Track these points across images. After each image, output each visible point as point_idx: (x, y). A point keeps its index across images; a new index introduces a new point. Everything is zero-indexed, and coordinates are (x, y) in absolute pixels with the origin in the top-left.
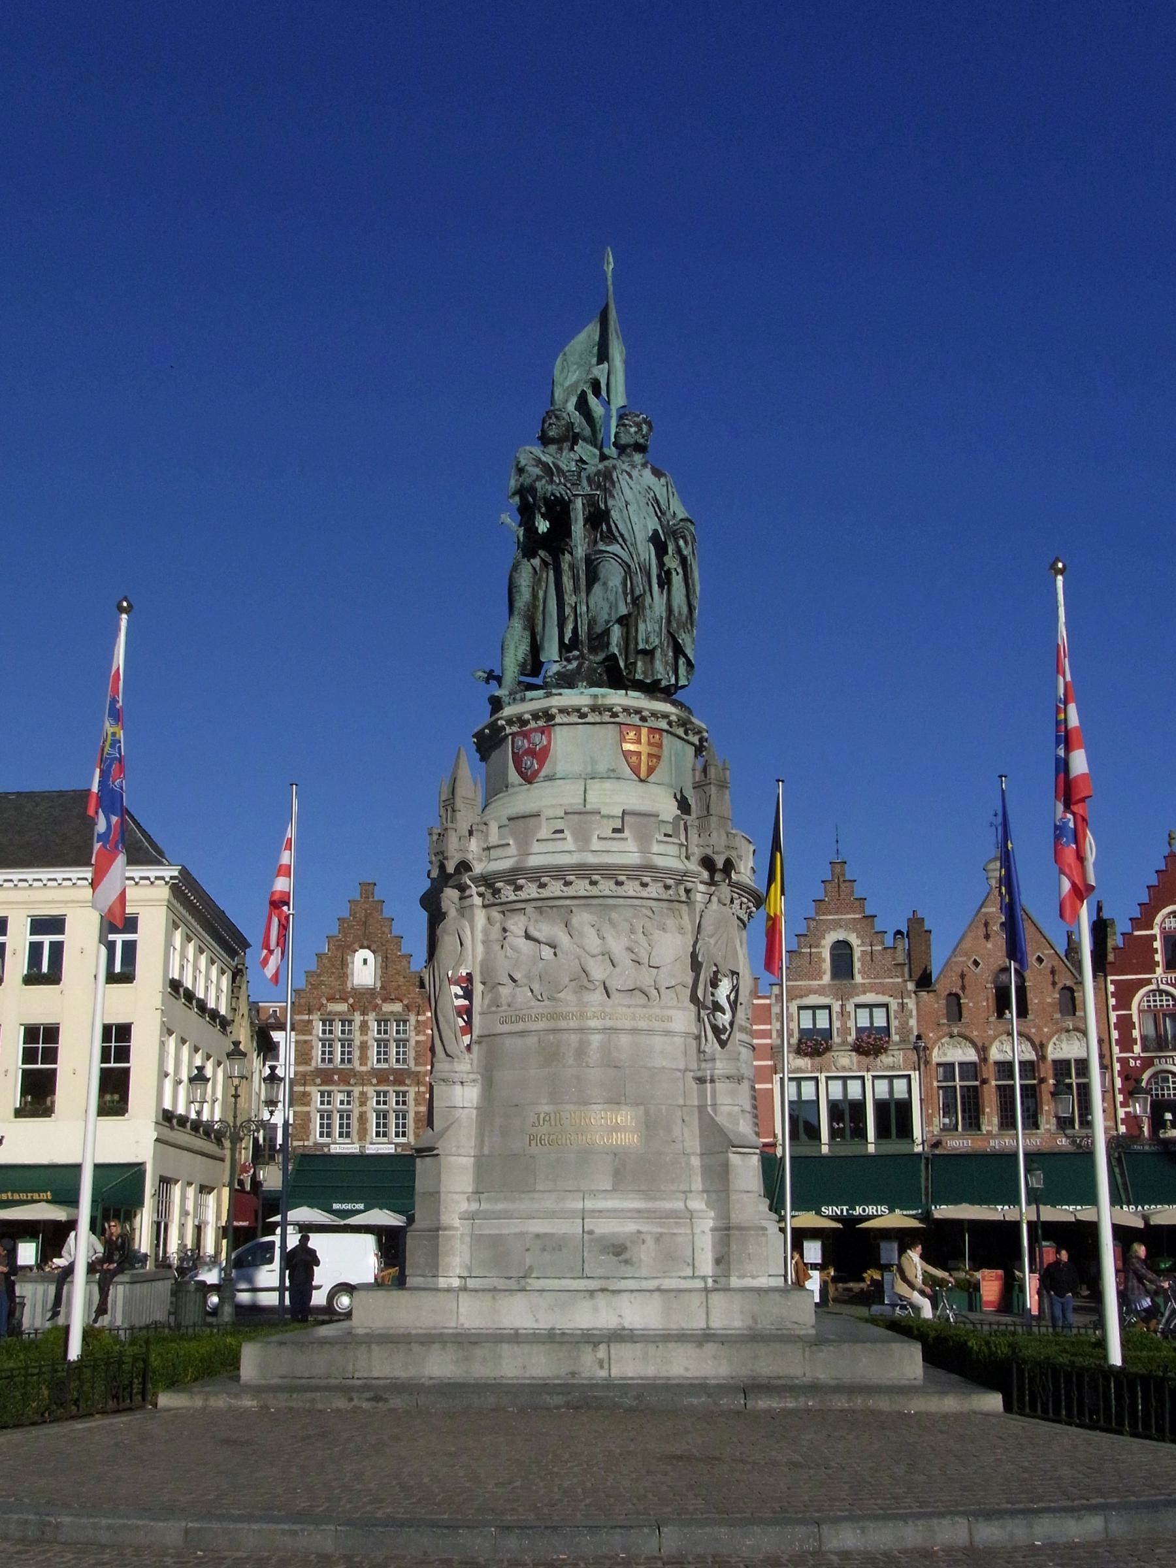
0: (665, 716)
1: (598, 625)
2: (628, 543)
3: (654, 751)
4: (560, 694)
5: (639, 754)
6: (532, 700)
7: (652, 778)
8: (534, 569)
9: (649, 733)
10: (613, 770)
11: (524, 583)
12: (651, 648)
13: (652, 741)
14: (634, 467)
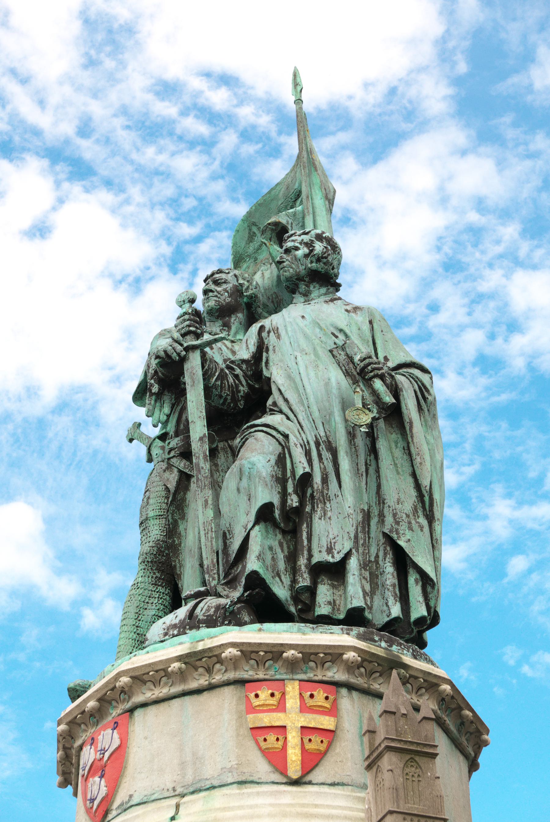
7: (317, 775)
10: (230, 771)
12: (338, 558)
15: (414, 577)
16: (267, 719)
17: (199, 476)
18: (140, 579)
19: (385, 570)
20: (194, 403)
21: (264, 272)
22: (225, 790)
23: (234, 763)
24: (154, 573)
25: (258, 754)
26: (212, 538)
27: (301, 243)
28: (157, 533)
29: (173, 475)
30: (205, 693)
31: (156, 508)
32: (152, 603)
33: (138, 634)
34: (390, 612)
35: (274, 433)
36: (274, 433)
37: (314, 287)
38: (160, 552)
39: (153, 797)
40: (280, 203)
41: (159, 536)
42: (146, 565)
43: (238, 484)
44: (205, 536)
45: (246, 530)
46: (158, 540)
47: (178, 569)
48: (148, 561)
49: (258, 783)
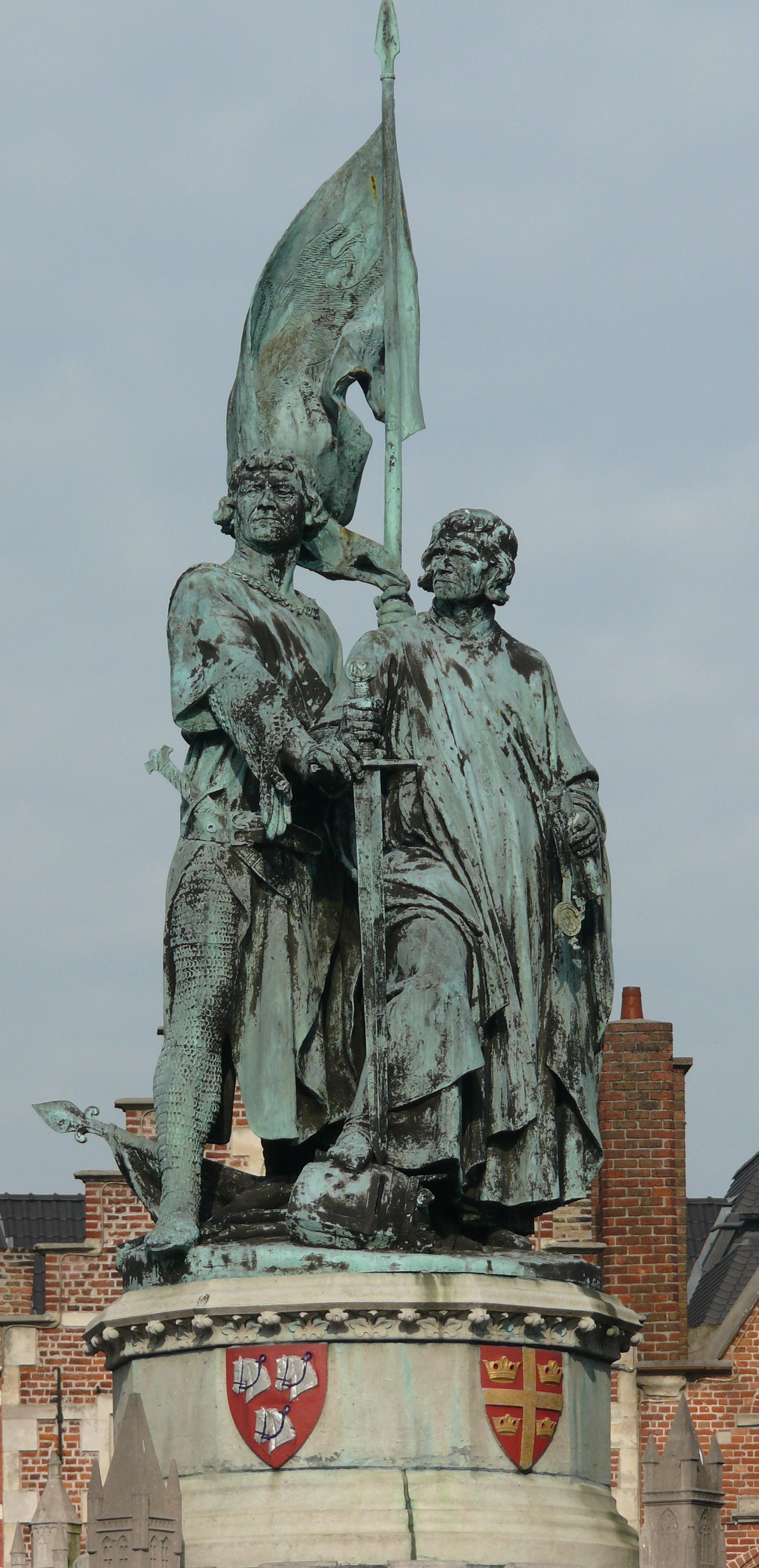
0: (570, 1319)
1: (411, 1079)
2: (467, 862)
3: (547, 1400)
4: (343, 1267)
5: (516, 1411)
6: (273, 1269)
8: (236, 901)
9: (540, 1360)
10: (463, 1452)
11: (213, 940)
12: (519, 1125)
13: (543, 1378)
14: (473, 652)
15: (576, 1139)
16: (503, 1397)
17: (371, 980)
18: (196, 1042)
19: (545, 1124)
20: (370, 861)
21: (294, 410)
22: (456, 1473)
23: (468, 1444)
24: (213, 1036)
25: (490, 1434)
26: (384, 1080)
27: (479, 549)
28: (223, 974)
29: (244, 879)
30: (429, 1345)
31: (220, 931)
32: (210, 1082)
33: (198, 1131)
34: (549, 1190)
35: (456, 918)
36: (456, 918)
37: (478, 616)
38: (224, 1005)
39: (366, 1464)
40: (307, 239)
41: (225, 979)
42: (206, 1023)
43: (428, 1012)
44: (376, 1075)
45: (435, 1085)
46: (225, 987)
47: (237, 1028)
48: (209, 1018)
49: (489, 1471)
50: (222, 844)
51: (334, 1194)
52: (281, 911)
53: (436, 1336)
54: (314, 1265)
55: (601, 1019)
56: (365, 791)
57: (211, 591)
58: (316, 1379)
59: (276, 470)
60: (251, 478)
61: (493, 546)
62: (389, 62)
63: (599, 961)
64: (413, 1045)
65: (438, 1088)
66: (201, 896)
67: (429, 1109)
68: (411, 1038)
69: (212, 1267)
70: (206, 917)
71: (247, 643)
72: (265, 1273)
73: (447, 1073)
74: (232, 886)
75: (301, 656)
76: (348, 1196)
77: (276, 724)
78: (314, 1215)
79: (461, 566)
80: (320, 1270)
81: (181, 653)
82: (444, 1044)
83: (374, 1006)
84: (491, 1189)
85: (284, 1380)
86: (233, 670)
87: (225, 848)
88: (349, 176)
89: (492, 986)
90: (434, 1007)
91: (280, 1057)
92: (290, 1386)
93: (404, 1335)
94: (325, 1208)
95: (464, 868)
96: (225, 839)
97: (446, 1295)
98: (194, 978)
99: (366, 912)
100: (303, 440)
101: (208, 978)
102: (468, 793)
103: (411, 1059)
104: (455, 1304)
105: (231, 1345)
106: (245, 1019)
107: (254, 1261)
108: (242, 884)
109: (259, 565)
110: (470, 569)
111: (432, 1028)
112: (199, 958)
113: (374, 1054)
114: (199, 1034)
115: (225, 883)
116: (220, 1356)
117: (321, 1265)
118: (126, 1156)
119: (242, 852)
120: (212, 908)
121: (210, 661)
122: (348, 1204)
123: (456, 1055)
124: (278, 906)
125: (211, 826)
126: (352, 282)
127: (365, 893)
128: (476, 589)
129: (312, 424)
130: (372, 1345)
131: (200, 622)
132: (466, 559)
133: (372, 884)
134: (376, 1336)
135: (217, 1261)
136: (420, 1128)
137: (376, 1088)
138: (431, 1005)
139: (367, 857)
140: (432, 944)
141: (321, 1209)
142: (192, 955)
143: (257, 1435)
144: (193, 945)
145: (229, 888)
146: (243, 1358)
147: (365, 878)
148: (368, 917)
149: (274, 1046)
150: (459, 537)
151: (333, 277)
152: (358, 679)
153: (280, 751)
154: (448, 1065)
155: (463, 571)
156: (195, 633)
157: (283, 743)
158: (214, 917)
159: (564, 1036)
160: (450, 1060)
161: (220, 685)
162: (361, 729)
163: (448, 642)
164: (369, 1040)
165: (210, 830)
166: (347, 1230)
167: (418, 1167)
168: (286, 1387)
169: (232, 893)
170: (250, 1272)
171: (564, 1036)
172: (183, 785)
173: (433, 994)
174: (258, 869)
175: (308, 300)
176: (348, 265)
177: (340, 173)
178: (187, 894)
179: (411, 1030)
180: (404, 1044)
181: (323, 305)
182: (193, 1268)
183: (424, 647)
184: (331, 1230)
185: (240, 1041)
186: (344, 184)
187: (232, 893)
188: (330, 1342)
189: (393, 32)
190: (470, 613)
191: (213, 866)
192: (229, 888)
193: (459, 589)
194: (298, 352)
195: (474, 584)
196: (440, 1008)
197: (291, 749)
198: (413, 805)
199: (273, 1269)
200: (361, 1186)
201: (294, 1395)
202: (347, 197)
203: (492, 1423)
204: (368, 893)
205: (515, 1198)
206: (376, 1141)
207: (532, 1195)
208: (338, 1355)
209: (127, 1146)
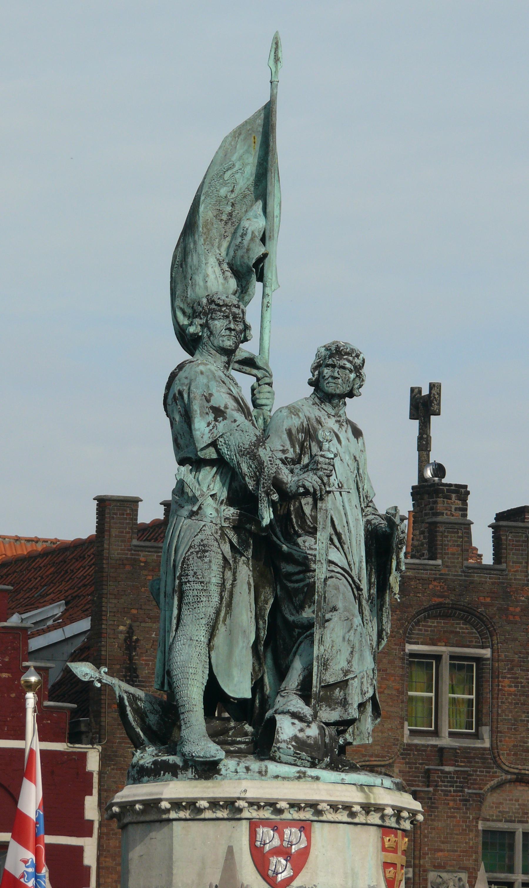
1: (330, 671)
2: (346, 547)
4: (317, 778)
5: (394, 865)
6: (277, 777)
11: (214, 580)
17: (320, 613)
18: (203, 639)
20: (324, 545)
23: (375, 884)
28: (217, 600)
29: (227, 546)
30: (359, 826)
43: (345, 634)
45: (345, 675)
50: (216, 524)
51: (300, 735)
52: (245, 566)
53: (364, 822)
54: (301, 776)
55: (383, 639)
56: (324, 505)
57: (215, 377)
58: (306, 842)
59: (234, 308)
60: (220, 311)
61: (359, 365)
62: (274, 73)
63: (387, 606)
64: (334, 652)
65: (347, 678)
66: (207, 554)
67: (338, 689)
68: (334, 648)
69: (237, 772)
70: (210, 567)
71: (239, 410)
72: (272, 779)
73: (353, 669)
74: (223, 550)
75: (250, 418)
76: (308, 737)
77: (270, 461)
78: (290, 746)
79: (344, 376)
80: (304, 779)
81: (198, 412)
82: (352, 652)
83: (320, 628)
84: (350, 735)
85: (289, 842)
86: (238, 426)
87: (218, 528)
88: (240, 134)
89: (367, 620)
90: (349, 632)
91: (244, 651)
92: (291, 845)
93: (349, 820)
94: (296, 743)
95: (343, 550)
96: (219, 522)
97: (375, 799)
98: (202, 601)
99: (320, 574)
100: (221, 288)
101: (210, 602)
102: (343, 506)
103: (332, 660)
104: (380, 805)
105: (252, 819)
106: (219, 627)
107: (266, 772)
108: (226, 548)
109: (220, 361)
110: (349, 378)
111: (346, 643)
112: (205, 590)
113: (318, 656)
114: (204, 634)
115: (220, 548)
116: (245, 825)
117: (305, 777)
118: (126, 698)
119: (227, 530)
120: (213, 562)
121: (220, 419)
122: (309, 742)
123: (359, 659)
124: (244, 563)
125: (211, 514)
126: (233, 196)
127: (320, 563)
128: (348, 389)
129: (225, 279)
130: (333, 824)
131: (211, 395)
132: (348, 371)
133: (324, 559)
134: (337, 820)
135: (241, 769)
136: (331, 699)
137: (317, 675)
138: (347, 630)
139: (322, 543)
140: (343, 594)
141: (294, 743)
142: (201, 588)
143: (270, 871)
144: (201, 582)
145: (221, 550)
146: (263, 827)
147: (320, 555)
148: (321, 577)
149: (241, 644)
150: (344, 359)
151: (223, 191)
152: (325, 441)
153: (274, 477)
154: (354, 665)
155: (345, 378)
156: (208, 401)
157: (275, 472)
158: (214, 567)
159: (373, 649)
160: (355, 662)
161: (229, 434)
162: (326, 470)
163: (329, 417)
164: (316, 647)
165: (210, 516)
166: (308, 756)
167: (332, 721)
168: (289, 846)
169: (223, 554)
170: (263, 778)
171: (373, 649)
172: (197, 489)
173: (349, 623)
174: (235, 541)
175: (210, 204)
176: (232, 186)
177: (235, 132)
178: (197, 552)
179: (334, 643)
180: (329, 651)
181: (217, 207)
182: (223, 772)
183: (317, 419)
184: (299, 756)
185: (215, 639)
186: (237, 139)
187: (223, 554)
188: (312, 821)
189: (280, 55)
190: (340, 402)
191: (213, 537)
192: (221, 550)
193: (342, 388)
194: (211, 235)
195: (349, 386)
196: (352, 632)
197: (281, 476)
198: (311, 510)
199: (277, 777)
200: (313, 731)
201: (293, 851)
202: (238, 146)
203: (385, 872)
204: (322, 563)
205: (357, 740)
206: (315, 705)
207: (368, 739)
208: (316, 829)
209: (126, 692)
